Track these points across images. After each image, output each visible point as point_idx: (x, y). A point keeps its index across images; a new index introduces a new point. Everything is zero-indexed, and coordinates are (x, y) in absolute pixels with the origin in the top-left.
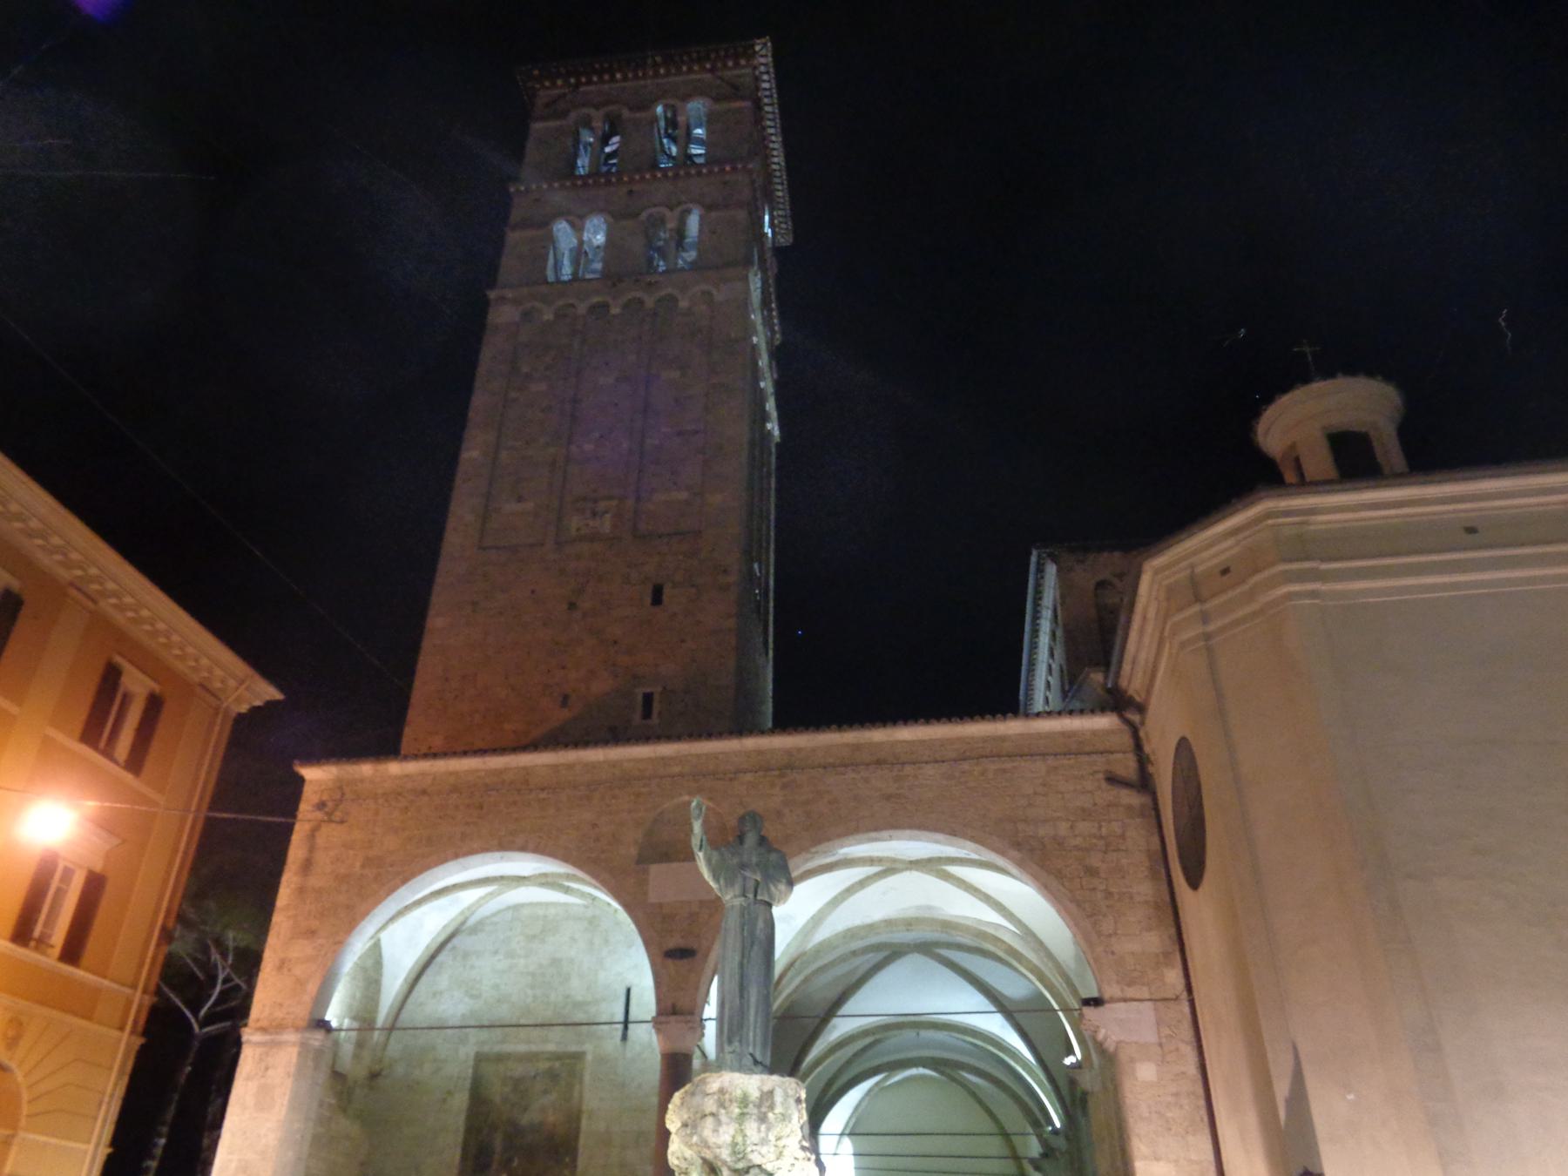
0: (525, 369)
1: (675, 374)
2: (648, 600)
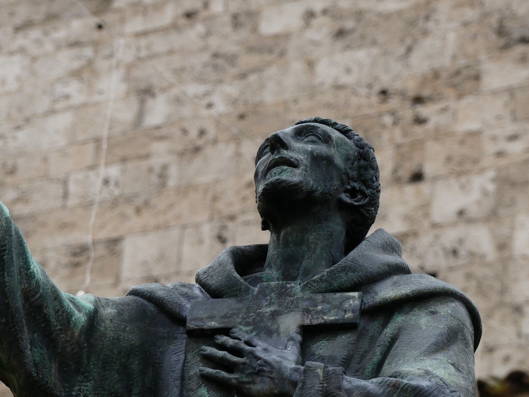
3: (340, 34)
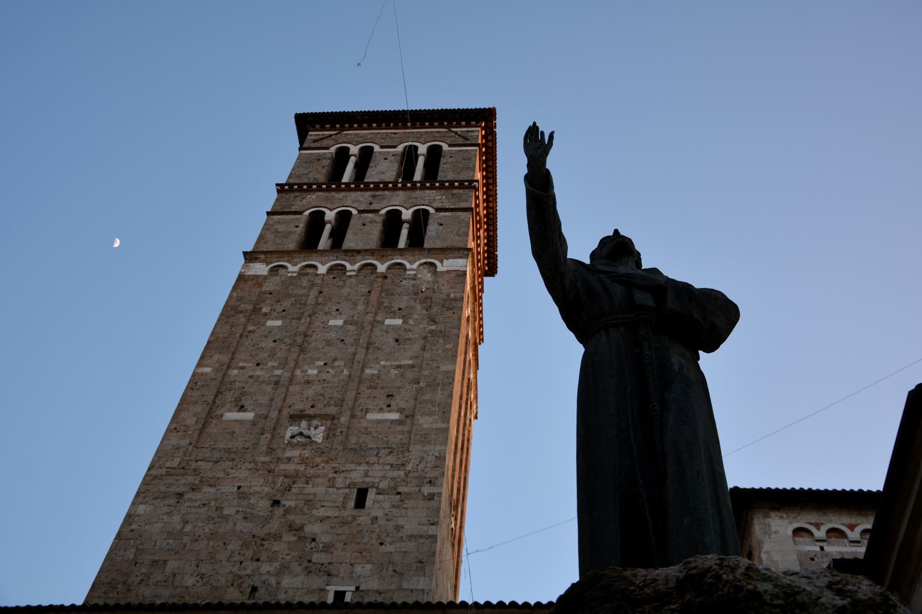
0: (264, 310)
1: (399, 322)
2: (352, 504)
3: (245, 518)
